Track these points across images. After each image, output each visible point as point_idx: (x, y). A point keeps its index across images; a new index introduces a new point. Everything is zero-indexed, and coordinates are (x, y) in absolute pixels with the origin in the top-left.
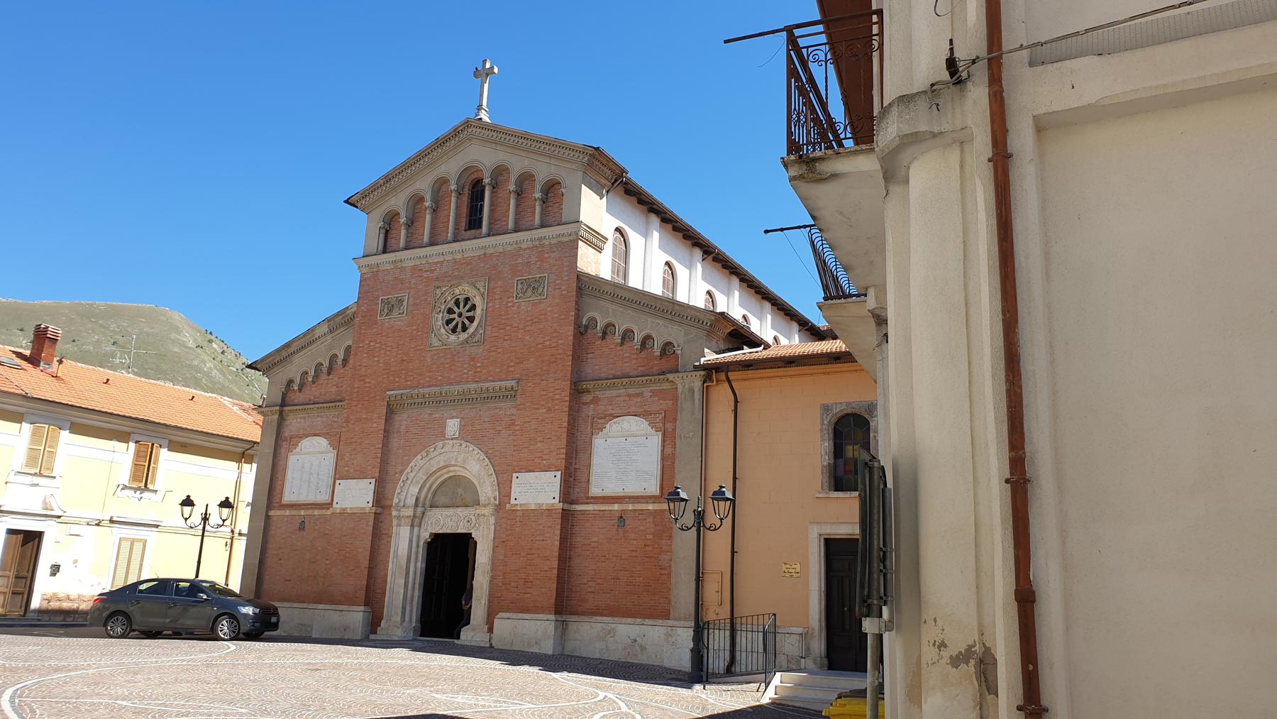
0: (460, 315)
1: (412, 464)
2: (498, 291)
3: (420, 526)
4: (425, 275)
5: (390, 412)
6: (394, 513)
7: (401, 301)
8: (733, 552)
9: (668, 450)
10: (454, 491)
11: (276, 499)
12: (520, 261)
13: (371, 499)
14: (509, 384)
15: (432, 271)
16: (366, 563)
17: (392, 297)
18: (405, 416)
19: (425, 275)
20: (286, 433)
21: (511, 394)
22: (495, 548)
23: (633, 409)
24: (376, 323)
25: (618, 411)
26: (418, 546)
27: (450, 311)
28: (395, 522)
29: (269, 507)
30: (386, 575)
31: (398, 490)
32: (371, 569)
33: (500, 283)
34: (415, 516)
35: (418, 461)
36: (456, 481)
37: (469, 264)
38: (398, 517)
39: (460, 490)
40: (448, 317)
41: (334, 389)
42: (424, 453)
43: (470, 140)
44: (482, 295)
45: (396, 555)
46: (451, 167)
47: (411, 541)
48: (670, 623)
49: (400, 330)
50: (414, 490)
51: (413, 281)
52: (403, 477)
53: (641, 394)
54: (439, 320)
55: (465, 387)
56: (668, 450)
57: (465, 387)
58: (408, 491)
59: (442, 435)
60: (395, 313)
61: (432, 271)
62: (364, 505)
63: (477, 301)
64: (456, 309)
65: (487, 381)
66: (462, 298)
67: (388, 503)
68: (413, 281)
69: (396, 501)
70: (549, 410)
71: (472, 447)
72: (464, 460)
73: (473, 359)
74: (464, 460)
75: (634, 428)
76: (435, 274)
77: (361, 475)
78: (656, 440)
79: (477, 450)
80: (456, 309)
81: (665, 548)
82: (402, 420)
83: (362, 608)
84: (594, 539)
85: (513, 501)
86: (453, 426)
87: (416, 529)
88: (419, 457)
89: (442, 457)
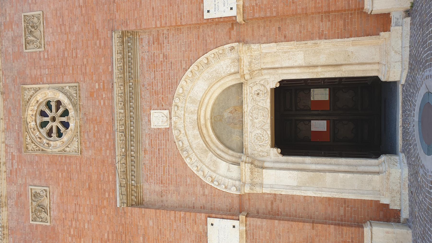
0: (54, 119)
1: (194, 169)
2: (34, 72)
3: (264, 162)
4: (15, 166)
5: (140, 204)
6: (247, 190)
7: (36, 195)
10: (226, 123)
12: (10, 50)
13: (230, 223)
14: (116, 41)
15: (13, 156)
16: (308, 226)
17: (31, 205)
18: (146, 186)
21: (129, 37)
22: (287, 39)
24: (53, 228)
26: (287, 162)
27: (49, 134)
28: (258, 190)
30: (322, 200)
31: (222, 188)
32: (313, 220)
33: (28, 72)
34: (252, 163)
35: (192, 163)
36: (217, 120)
37: (10, 113)
38: (253, 184)
39: (226, 114)
40: (54, 135)
42: (184, 155)
44: (36, 90)
45: (298, 187)
47: (281, 169)
49: (62, 195)
50: (223, 166)
51: (20, 181)
52: (208, 181)
54: (56, 145)
55: (117, 99)
57: (117, 99)
58: (223, 175)
59: (166, 132)
60: (46, 202)
61: (13, 156)
62: (236, 233)
63: (41, 97)
64: (46, 119)
65: (112, 73)
66: (40, 119)
67: (236, 205)
68: (20, 181)
69: (233, 191)
71: (179, 90)
72: (193, 101)
73: (92, 95)
74: (193, 101)
76: (16, 153)
79: (182, 82)
80: (46, 119)
82: (150, 189)
83: (367, 230)
85: (233, 13)
86: (158, 119)
87: (266, 164)
88: (187, 161)
89: (189, 133)
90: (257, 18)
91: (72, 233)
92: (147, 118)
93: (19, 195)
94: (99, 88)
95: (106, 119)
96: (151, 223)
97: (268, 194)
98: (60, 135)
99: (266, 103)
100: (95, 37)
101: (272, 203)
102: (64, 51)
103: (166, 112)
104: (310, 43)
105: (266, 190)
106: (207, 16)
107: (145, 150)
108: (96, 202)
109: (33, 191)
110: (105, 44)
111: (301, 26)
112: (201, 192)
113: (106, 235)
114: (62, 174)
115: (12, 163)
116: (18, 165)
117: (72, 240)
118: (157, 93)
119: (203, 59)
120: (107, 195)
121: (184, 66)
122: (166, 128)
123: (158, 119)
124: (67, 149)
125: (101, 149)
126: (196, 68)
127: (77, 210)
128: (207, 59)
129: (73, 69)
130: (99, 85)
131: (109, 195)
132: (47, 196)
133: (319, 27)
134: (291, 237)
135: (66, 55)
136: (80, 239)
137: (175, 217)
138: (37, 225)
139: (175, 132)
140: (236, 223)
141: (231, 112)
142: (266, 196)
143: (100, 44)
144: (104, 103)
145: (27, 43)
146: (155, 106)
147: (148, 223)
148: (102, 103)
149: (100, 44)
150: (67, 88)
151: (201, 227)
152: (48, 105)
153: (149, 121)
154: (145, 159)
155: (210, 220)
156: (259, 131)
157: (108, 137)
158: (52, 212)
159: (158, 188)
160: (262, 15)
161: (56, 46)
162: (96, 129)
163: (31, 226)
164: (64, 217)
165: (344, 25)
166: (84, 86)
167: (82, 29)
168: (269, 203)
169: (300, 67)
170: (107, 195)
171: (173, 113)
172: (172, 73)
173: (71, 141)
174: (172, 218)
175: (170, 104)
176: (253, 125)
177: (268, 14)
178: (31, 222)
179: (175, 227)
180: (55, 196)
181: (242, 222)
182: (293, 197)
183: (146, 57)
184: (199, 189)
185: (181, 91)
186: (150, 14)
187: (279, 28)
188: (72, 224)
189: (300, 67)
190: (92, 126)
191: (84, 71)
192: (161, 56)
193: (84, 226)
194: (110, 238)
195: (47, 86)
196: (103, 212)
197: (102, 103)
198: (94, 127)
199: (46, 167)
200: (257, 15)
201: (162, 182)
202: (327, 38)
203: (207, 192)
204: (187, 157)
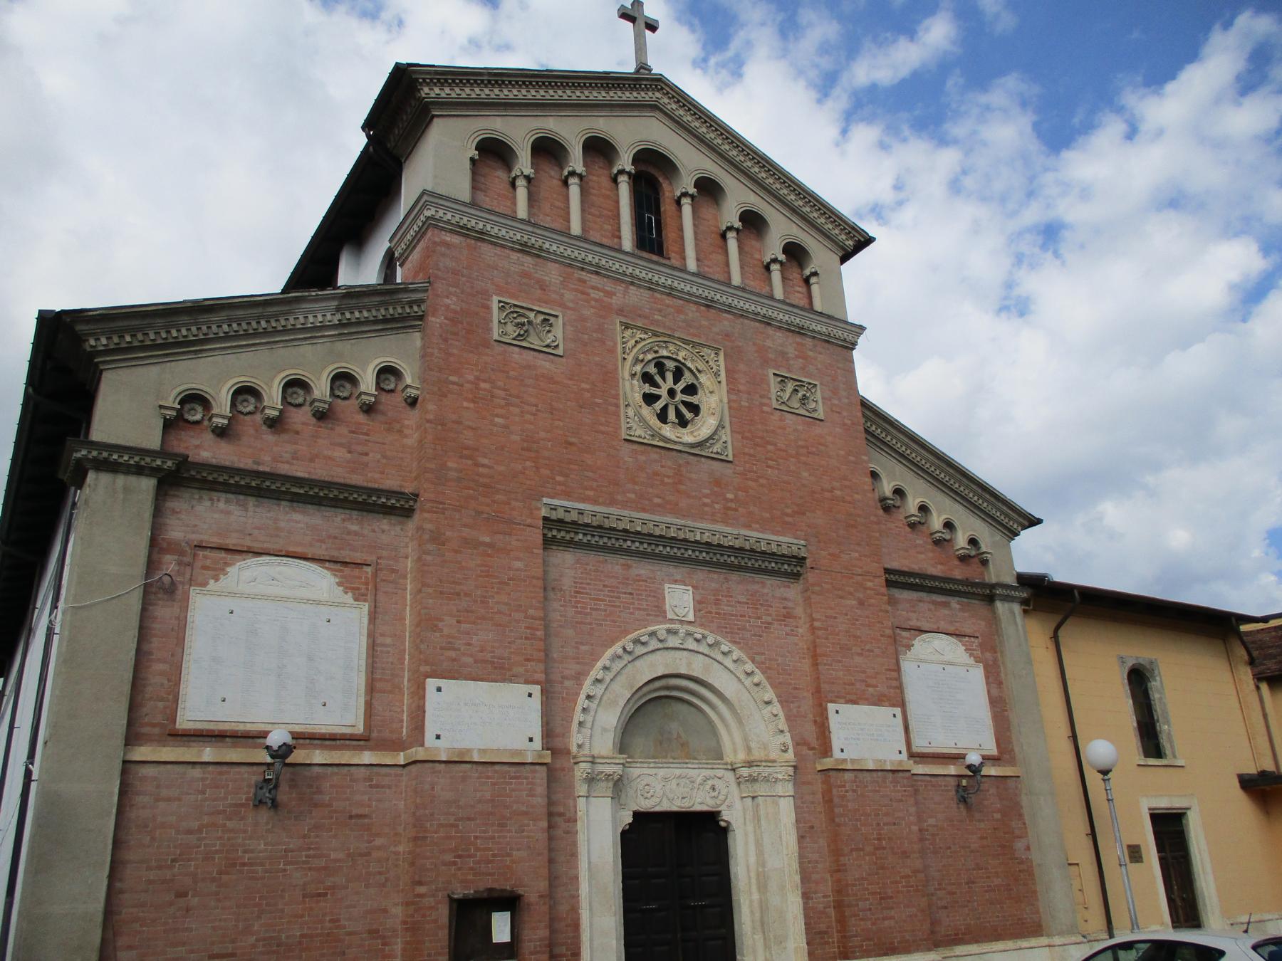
0: (672, 393)
4: (595, 294)
8: (1093, 834)
9: (995, 692)
11: (152, 711)
19: (595, 294)
20: (175, 532)
22: (801, 838)
23: (943, 625)
25: (926, 626)
29: (132, 737)
30: (575, 910)
41: (340, 453)
43: (655, 107)
46: (630, 133)
48: (1057, 940)
49: (551, 380)
53: (946, 605)
56: (995, 692)
59: (659, 612)
62: (519, 743)
70: (861, 603)
73: (717, 483)
75: (949, 657)
77: (497, 671)
78: (978, 673)
81: (1017, 832)
84: (931, 821)
85: (837, 754)
90: (830, 791)
91: (483, 385)
92: (679, 577)
93: (543, 287)
94: (727, 500)
95: (684, 503)
96: (518, 564)
97: (575, 807)
98: (650, 399)
99: (700, 802)
100: (796, 509)
101: (561, 815)
102: (775, 445)
103: (691, 617)
104: (797, 878)
105: (581, 802)
106: (831, 707)
107: (629, 567)
108: (546, 454)
109: (552, 320)
110: (787, 523)
111: (817, 862)
112: (567, 672)
113: (486, 461)
114: (588, 391)
115: (598, 289)
116: (596, 300)
117: (468, 382)
118: (717, 602)
119: (769, 694)
120: (559, 478)
121: (758, 658)
122: (665, 612)
123: (680, 598)
124: (631, 412)
125: (635, 483)
126: (756, 680)
127: (527, 408)
128: (768, 703)
129: (750, 455)
130: (732, 500)
131: (560, 483)
132: (548, 346)
133: (815, 892)
134: (523, 854)
135: (770, 447)
136: (474, 402)
137: (533, 618)
138: (488, 308)
139: (661, 628)
140: (537, 744)
141: (679, 736)
142: (571, 802)
143: (787, 515)
144: (705, 505)
145: (783, 380)
146: (698, 598)
147: (518, 559)
148: (706, 500)
149: (787, 515)
150: (724, 438)
151: (521, 670)
152: (660, 366)
153: (675, 582)
154: (615, 565)
155: (536, 690)
156: (658, 787)
157: (657, 500)
158: (516, 349)
159: (567, 583)
160: (836, 800)
161: (779, 431)
162: (666, 480)
163: (486, 295)
164: (512, 373)
165: (820, 933)
166: (728, 470)
167: (804, 486)
168: (561, 809)
169: (762, 863)
170: (559, 478)
171: (691, 628)
172: (748, 635)
173: (647, 426)
174: (531, 612)
175: (702, 625)
176: (666, 779)
177: (836, 810)
178: (495, 299)
179: (517, 616)
180: (547, 365)
181: (540, 756)
182: (574, 855)
183: (766, 591)
184: (573, 668)
185: (725, 648)
186: (830, 612)
187: (812, 827)
188: (499, 388)
189: (762, 863)
190: (671, 473)
191: (750, 475)
192: (769, 619)
193: (497, 416)
194: (481, 470)
195: (725, 400)
196: (528, 464)
197: (706, 500)
198: (669, 477)
199: (597, 359)
200: (835, 791)
201: (577, 592)
202: (805, 904)
203: (567, 683)
204: (624, 649)
